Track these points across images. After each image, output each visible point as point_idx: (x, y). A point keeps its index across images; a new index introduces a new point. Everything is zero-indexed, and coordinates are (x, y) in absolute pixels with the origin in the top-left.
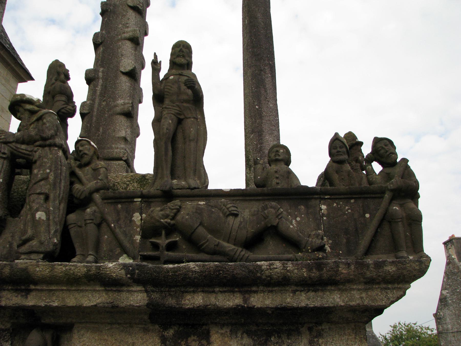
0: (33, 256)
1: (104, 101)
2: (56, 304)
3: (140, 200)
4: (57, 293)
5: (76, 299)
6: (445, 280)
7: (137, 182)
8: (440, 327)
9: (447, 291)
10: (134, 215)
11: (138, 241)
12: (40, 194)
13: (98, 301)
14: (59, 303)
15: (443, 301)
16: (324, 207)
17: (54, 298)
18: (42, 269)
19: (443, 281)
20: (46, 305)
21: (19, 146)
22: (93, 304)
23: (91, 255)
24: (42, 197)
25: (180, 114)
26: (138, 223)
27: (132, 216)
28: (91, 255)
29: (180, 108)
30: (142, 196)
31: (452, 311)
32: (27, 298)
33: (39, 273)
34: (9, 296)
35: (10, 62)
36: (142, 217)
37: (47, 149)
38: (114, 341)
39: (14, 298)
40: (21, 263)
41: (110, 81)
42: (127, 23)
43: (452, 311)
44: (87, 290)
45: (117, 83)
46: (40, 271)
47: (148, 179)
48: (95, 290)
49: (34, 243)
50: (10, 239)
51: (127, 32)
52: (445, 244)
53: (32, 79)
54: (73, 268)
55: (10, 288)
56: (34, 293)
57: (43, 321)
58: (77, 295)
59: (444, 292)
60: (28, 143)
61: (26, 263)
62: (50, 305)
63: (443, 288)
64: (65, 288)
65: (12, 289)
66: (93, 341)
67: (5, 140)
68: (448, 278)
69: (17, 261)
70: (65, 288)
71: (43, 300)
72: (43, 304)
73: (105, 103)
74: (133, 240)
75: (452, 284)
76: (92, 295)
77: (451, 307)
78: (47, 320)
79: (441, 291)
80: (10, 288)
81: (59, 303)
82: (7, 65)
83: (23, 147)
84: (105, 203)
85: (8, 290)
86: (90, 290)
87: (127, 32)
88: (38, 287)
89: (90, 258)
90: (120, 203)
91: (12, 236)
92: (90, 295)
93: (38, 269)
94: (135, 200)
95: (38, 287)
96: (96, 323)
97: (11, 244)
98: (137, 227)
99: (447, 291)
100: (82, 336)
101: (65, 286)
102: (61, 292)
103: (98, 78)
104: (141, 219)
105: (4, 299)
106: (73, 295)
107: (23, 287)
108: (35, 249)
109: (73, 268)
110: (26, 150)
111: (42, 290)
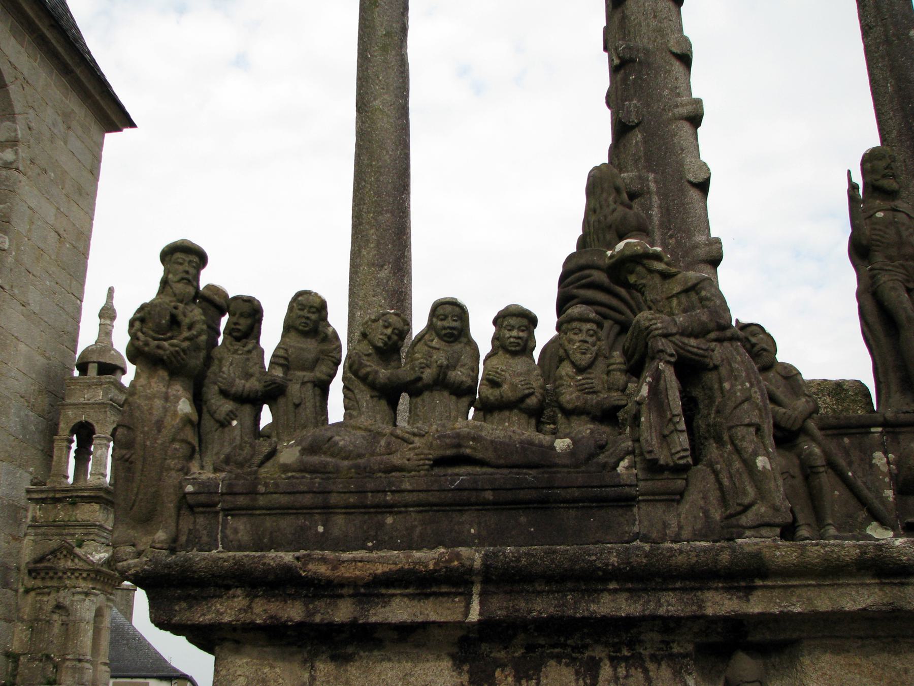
0: (764, 531)
1: (671, 237)
2: (797, 609)
3: (880, 429)
4: (798, 591)
5: (831, 599)
7: (829, 395)
10: (874, 455)
11: (891, 499)
12: (749, 425)
13: (868, 601)
14: (804, 607)
17: (794, 599)
18: (786, 552)
20: (781, 612)
21: (686, 340)
22: (860, 607)
23: (830, 524)
24: (752, 430)
25: (908, 281)
26: (885, 469)
27: (872, 458)
28: (830, 524)
29: (907, 270)
30: (885, 424)
32: (748, 601)
33: (780, 560)
34: (718, 598)
35: (93, 91)
36: (887, 458)
37: (726, 344)
38: (872, 667)
39: (726, 602)
40: (747, 543)
41: (674, 200)
42: (676, 88)
44: (848, 585)
45: (688, 204)
46: (782, 556)
47: (847, 390)
48: (862, 585)
49: (761, 509)
50: (702, 503)
51: (682, 105)
53: (132, 125)
54: (836, 549)
55: (720, 585)
56: (759, 593)
57: (749, 638)
58: (832, 593)
60: (696, 337)
61: (757, 544)
62: (789, 611)
64: (813, 583)
65: (722, 588)
66: (838, 667)
67: (665, 331)
69: (739, 541)
70: (813, 583)
71: (776, 603)
72: (776, 610)
73: (674, 240)
74: (882, 497)
76: (857, 592)
78: (756, 637)
80: (720, 585)
81: (804, 607)
83: (693, 342)
84: (828, 435)
85: (716, 589)
86: (855, 585)
87: (682, 105)
88: (770, 583)
90: (846, 435)
91: (703, 498)
92: (853, 593)
93: (778, 553)
94: (873, 430)
95: (769, 583)
96: (837, 637)
97: (706, 513)
98: (885, 475)
100: (817, 659)
101: (813, 579)
102: (805, 589)
103: (649, 192)
104: (888, 463)
105: (709, 604)
106: (825, 594)
107: (743, 584)
108: (767, 519)
109: (836, 549)
110: (698, 348)
111: (773, 587)
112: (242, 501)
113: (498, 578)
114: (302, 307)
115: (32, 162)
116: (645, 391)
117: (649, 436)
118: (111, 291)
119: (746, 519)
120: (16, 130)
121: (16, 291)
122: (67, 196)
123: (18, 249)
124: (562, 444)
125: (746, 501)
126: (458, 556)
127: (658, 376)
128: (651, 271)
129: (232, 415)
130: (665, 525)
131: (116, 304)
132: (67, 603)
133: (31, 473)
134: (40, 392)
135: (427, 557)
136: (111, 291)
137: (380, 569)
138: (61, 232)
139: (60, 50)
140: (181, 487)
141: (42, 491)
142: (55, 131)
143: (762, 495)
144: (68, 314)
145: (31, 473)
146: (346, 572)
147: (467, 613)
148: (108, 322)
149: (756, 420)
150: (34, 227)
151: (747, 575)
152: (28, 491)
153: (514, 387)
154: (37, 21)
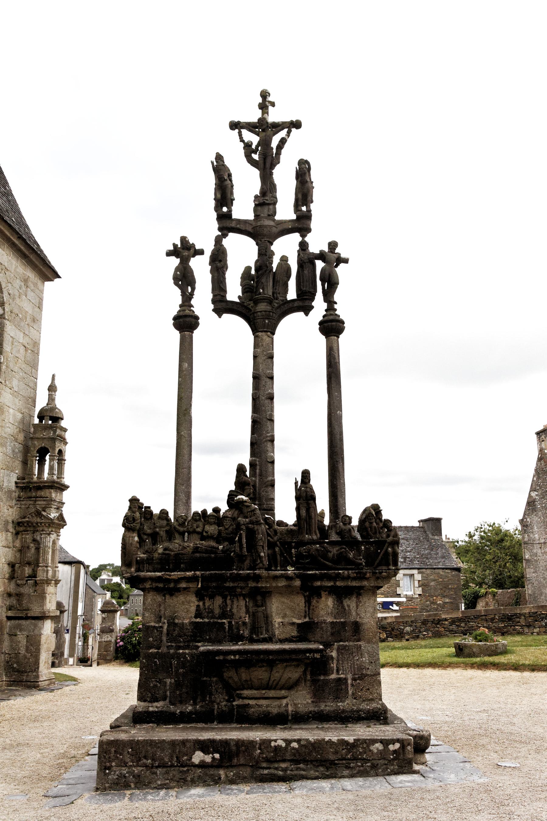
6: (535, 479)
8: (526, 536)
9: (537, 493)
15: (531, 504)
16: (363, 547)
19: (533, 480)
31: (540, 517)
35: (38, 265)
40: (257, 572)
43: (540, 517)
52: (538, 434)
53: (59, 277)
59: (534, 494)
60: (251, 524)
63: (532, 489)
68: (538, 478)
75: (543, 485)
77: (540, 513)
79: (530, 492)
82: (34, 267)
83: (250, 525)
89: (279, 568)
99: (537, 493)
103: (256, 465)
112: (150, 561)
113: (204, 578)
114: (163, 513)
115: (11, 312)
116: (237, 539)
117: (238, 549)
118: (54, 376)
119: (257, 567)
120: (3, 297)
121: (7, 382)
122: (28, 325)
123: (7, 360)
124: (221, 547)
125: (257, 563)
126: (196, 574)
127: (241, 534)
128: (244, 505)
129: (147, 539)
130: (241, 567)
131: (57, 383)
132: (38, 538)
133: (17, 474)
134: (20, 431)
135: (189, 574)
136: (54, 376)
137: (179, 576)
138: (26, 345)
139: (22, 248)
140: (136, 559)
141: (23, 483)
142: (21, 291)
143: (262, 562)
144: (31, 388)
145: (17, 474)
146: (172, 577)
147: (198, 585)
148: (53, 393)
149: (262, 544)
150: (14, 346)
151: (257, 578)
152: (16, 483)
153: (211, 534)
154: (11, 237)
